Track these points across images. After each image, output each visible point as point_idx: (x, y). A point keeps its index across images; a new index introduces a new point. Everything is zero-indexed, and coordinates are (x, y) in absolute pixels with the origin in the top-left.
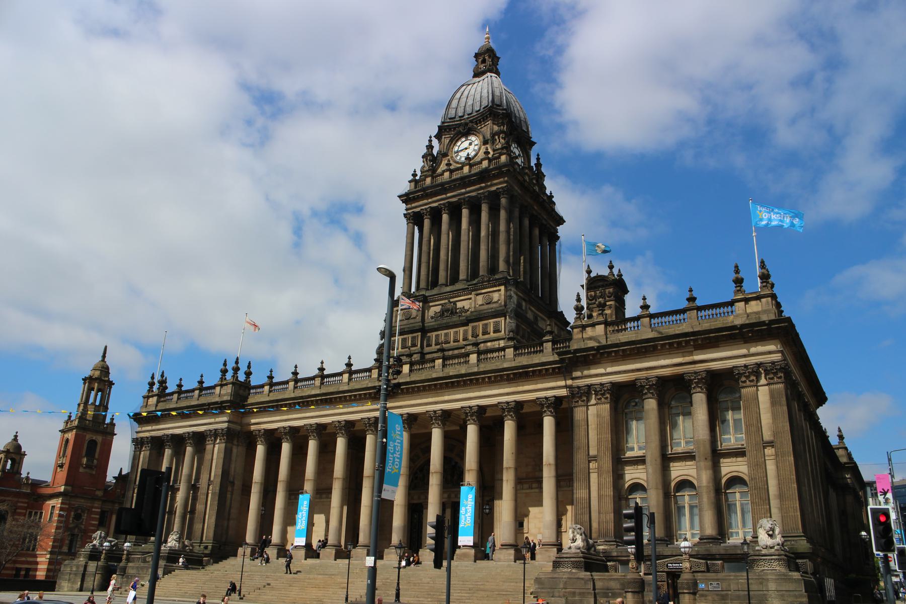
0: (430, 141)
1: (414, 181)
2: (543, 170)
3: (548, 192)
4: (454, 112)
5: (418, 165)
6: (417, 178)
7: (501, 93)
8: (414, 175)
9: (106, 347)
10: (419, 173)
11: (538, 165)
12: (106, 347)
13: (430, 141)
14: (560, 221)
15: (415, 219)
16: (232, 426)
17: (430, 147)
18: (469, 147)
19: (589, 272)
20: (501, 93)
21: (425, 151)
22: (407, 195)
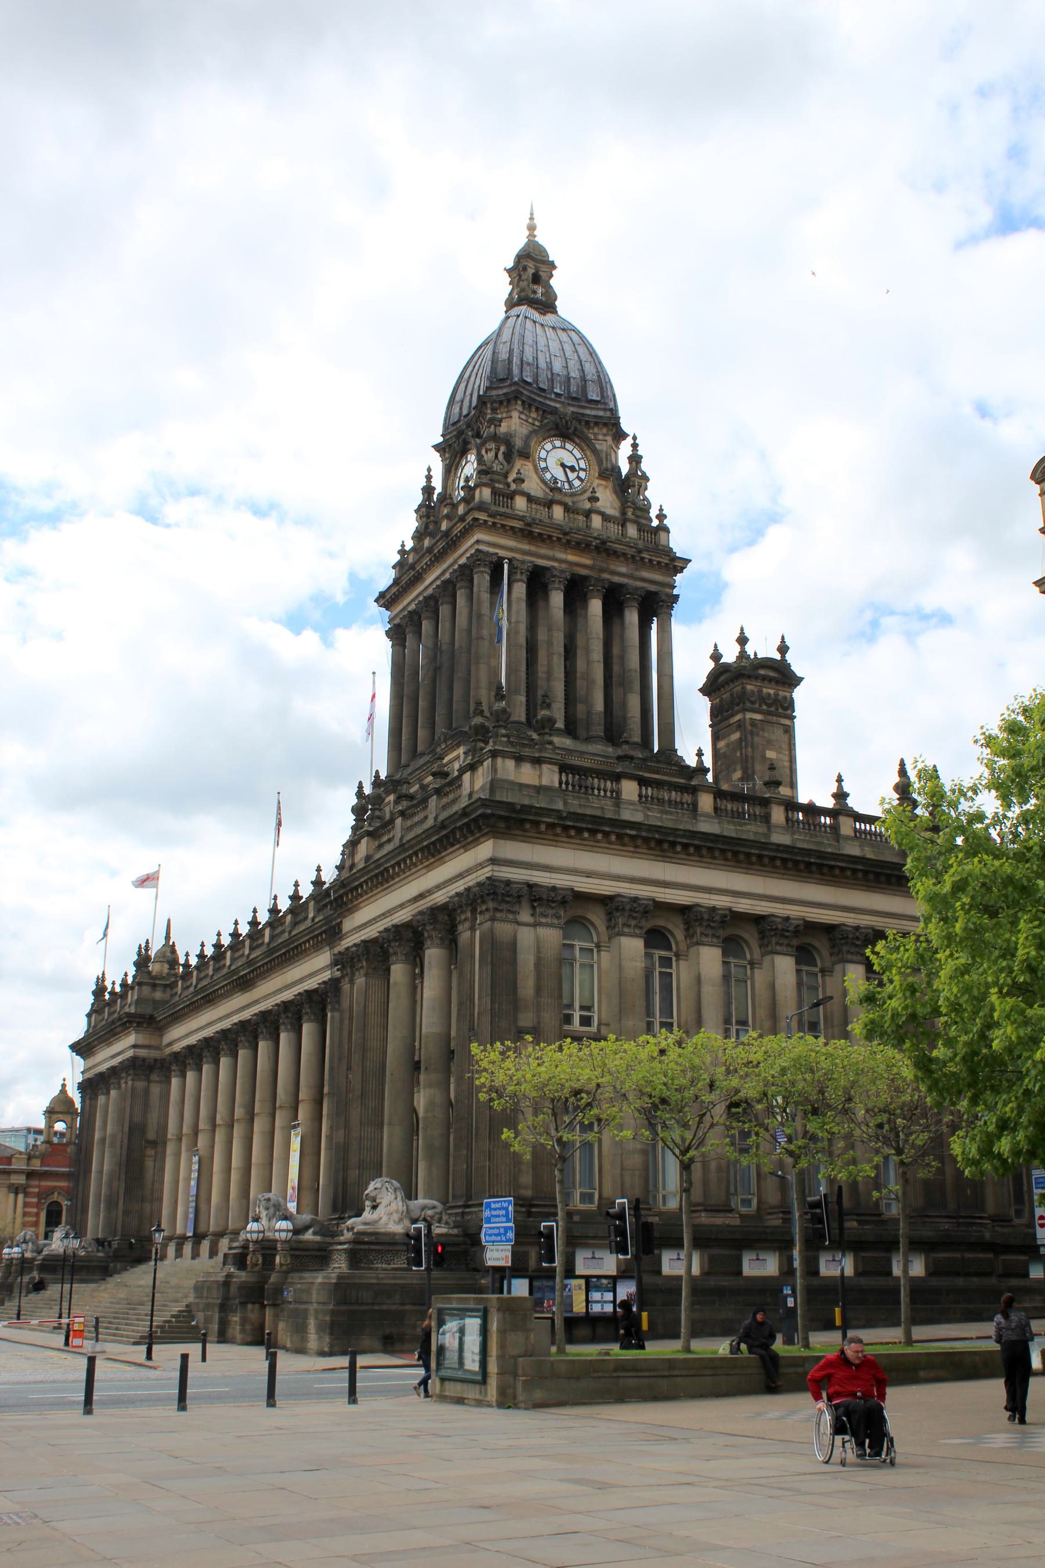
0: (429, 478)
2: (644, 466)
3: (654, 513)
4: (456, 409)
5: (404, 529)
7: (511, 351)
9: (169, 921)
11: (635, 459)
12: (169, 921)
13: (429, 478)
14: (676, 565)
15: (397, 634)
16: (142, 1053)
17: (428, 490)
19: (716, 656)
20: (511, 351)
21: (419, 498)
22: (382, 595)
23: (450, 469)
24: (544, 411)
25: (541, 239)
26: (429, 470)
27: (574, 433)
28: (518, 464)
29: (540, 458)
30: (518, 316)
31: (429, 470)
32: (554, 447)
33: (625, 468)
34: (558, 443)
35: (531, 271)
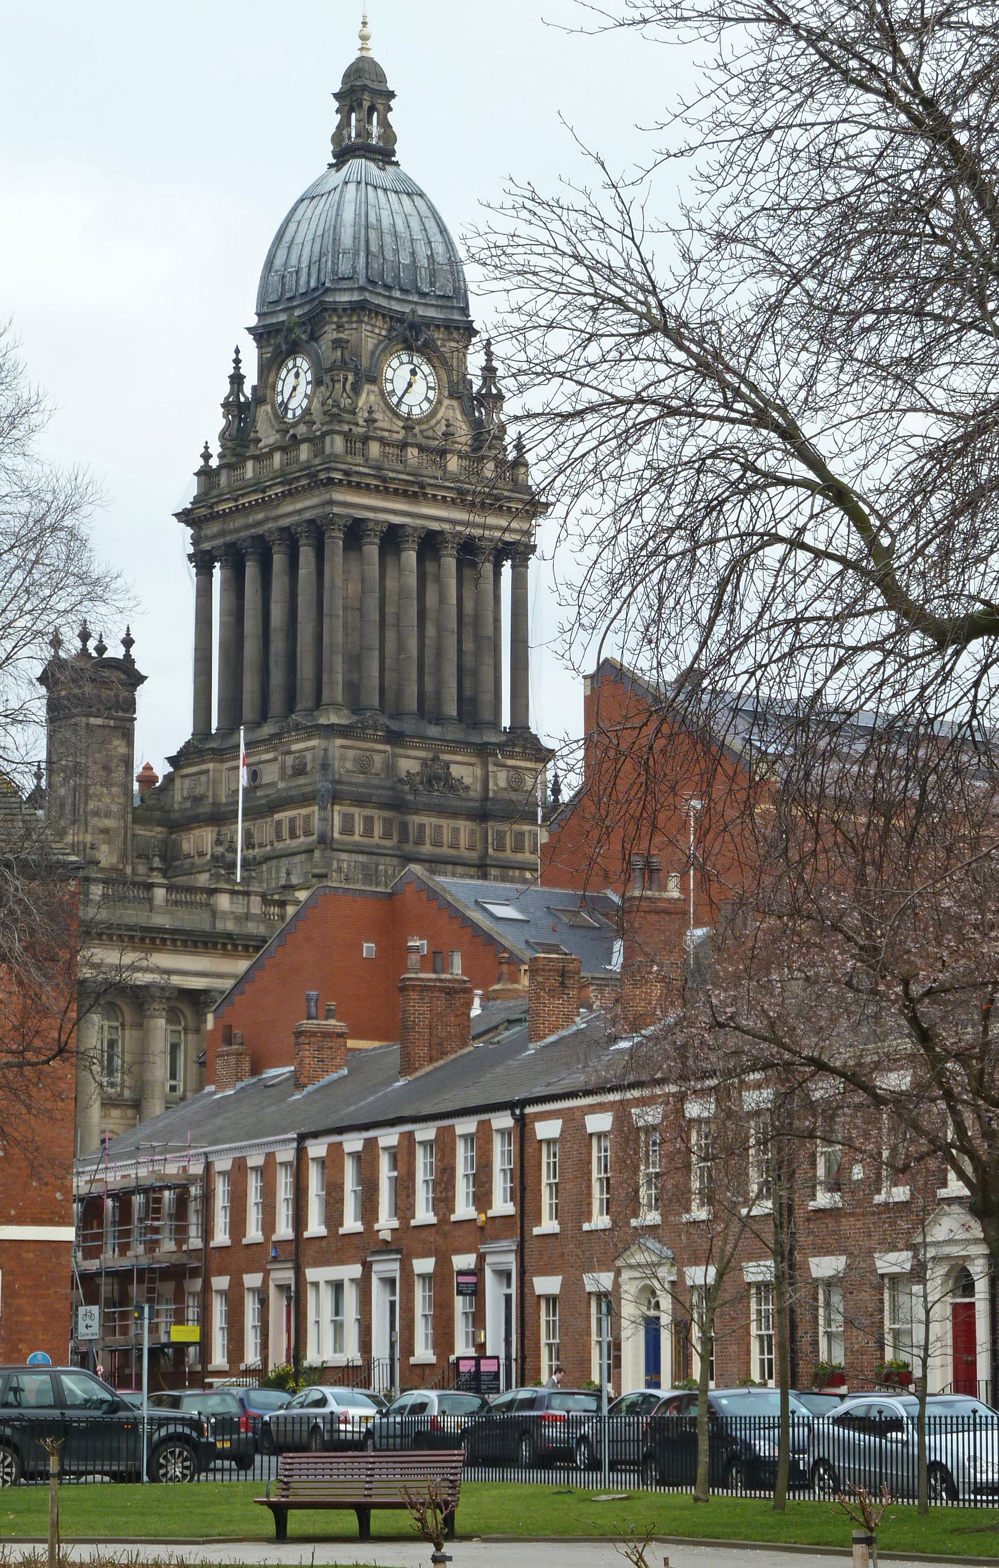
0: (237, 361)
1: (205, 473)
6: (214, 463)
8: (206, 456)
10: (215, 449)
11: (489, 372)
13: (237, 361)
15: (202, 561)
17: (237, 379)
18: (296, 386)
21: (225, 388)
23: (269, 368)
24: (391, 318)
25: (377, 54)
26: (237, 351)
27: (426, 344)
28: (367, 387)
29: (386, 379)
30: (359, 183)
31: (237, 351)
32: (402, 363)
33: (477, 384)
34: (405, 358)
35: (366, 104)
